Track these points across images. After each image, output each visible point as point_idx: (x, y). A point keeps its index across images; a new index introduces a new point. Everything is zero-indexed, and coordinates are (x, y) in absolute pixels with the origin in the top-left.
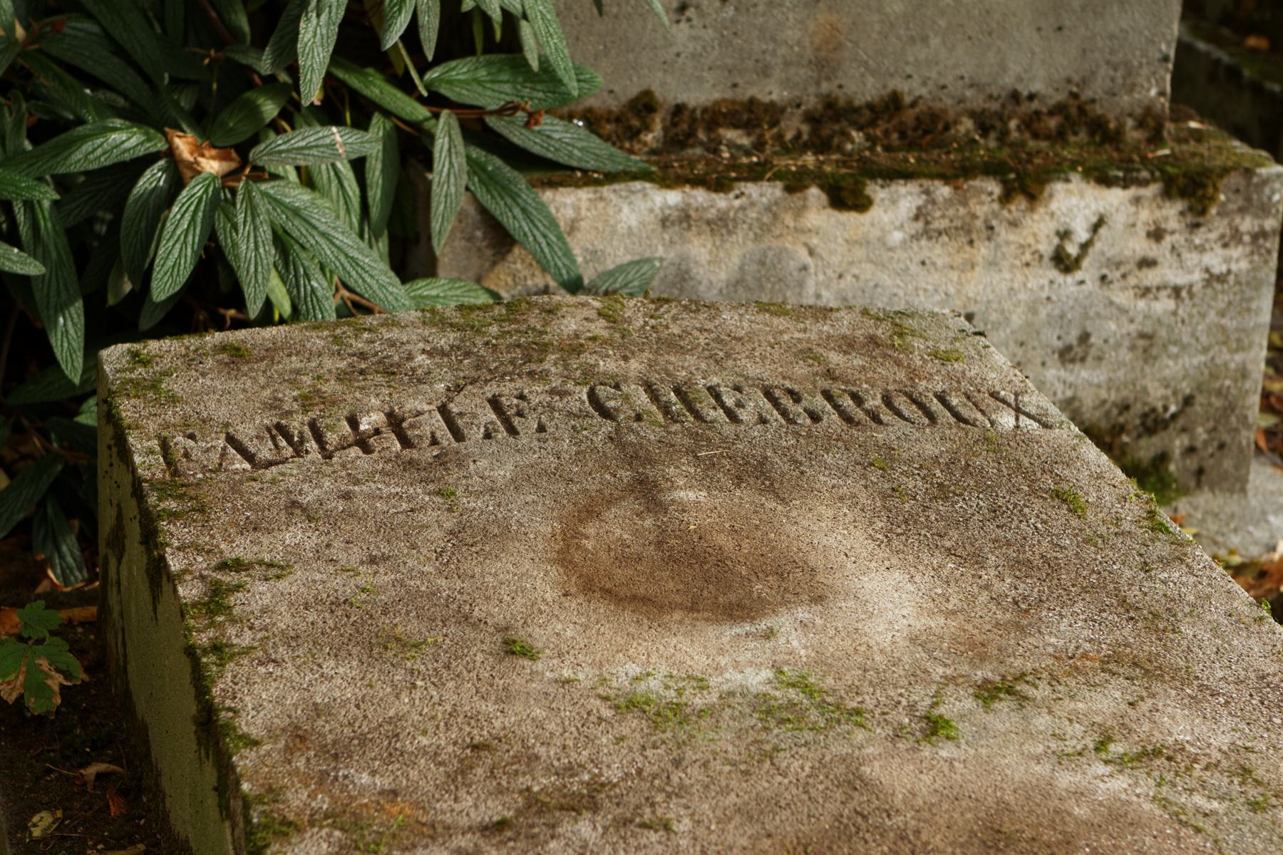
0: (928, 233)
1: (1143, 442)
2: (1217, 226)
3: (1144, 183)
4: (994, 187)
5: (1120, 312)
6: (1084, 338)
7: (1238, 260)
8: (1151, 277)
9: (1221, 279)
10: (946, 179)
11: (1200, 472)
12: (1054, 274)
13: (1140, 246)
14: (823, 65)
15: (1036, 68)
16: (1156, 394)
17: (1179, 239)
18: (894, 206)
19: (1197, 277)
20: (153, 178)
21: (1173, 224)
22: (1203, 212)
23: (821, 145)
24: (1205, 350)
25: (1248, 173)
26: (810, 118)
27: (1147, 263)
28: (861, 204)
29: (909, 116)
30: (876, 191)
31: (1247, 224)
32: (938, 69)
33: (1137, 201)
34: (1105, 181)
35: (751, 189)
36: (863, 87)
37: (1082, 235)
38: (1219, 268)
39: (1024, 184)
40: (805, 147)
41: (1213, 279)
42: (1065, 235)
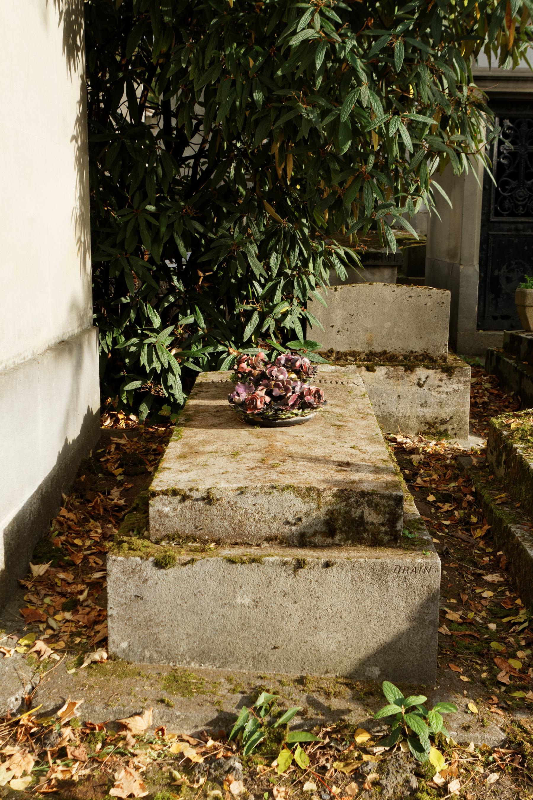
0: (388, 377)
1: (442, 426)
2: (455, 379)
3: (437, 369)
7: (461, 387)
8: (440, 389)
9: (457, 391)
10: (392, 366)
11: (455, 434)
12: (418, 387)
13: (438, 383)
15: (417, 346)
16: (444, 416)
18: (381, 371)
19: (451, 390)
20: (224, 355)
21: (445, 378)
22: (451, 376)
23: (369, 361)
24: (455, 406)
25: (462, 368)
26: (366, 355)
27: (439, 386)
28: (374, 371)
30: (376, 368)
31: (462, 379)
33: (436, 373)
34: (428, 368)
35: (350, 366)
36: (378, 349)
37: (424, 380)
38: (456, 388)
39: (410, 368)
40: (366, 361)
41: (455, 391)
42: (420, 379)
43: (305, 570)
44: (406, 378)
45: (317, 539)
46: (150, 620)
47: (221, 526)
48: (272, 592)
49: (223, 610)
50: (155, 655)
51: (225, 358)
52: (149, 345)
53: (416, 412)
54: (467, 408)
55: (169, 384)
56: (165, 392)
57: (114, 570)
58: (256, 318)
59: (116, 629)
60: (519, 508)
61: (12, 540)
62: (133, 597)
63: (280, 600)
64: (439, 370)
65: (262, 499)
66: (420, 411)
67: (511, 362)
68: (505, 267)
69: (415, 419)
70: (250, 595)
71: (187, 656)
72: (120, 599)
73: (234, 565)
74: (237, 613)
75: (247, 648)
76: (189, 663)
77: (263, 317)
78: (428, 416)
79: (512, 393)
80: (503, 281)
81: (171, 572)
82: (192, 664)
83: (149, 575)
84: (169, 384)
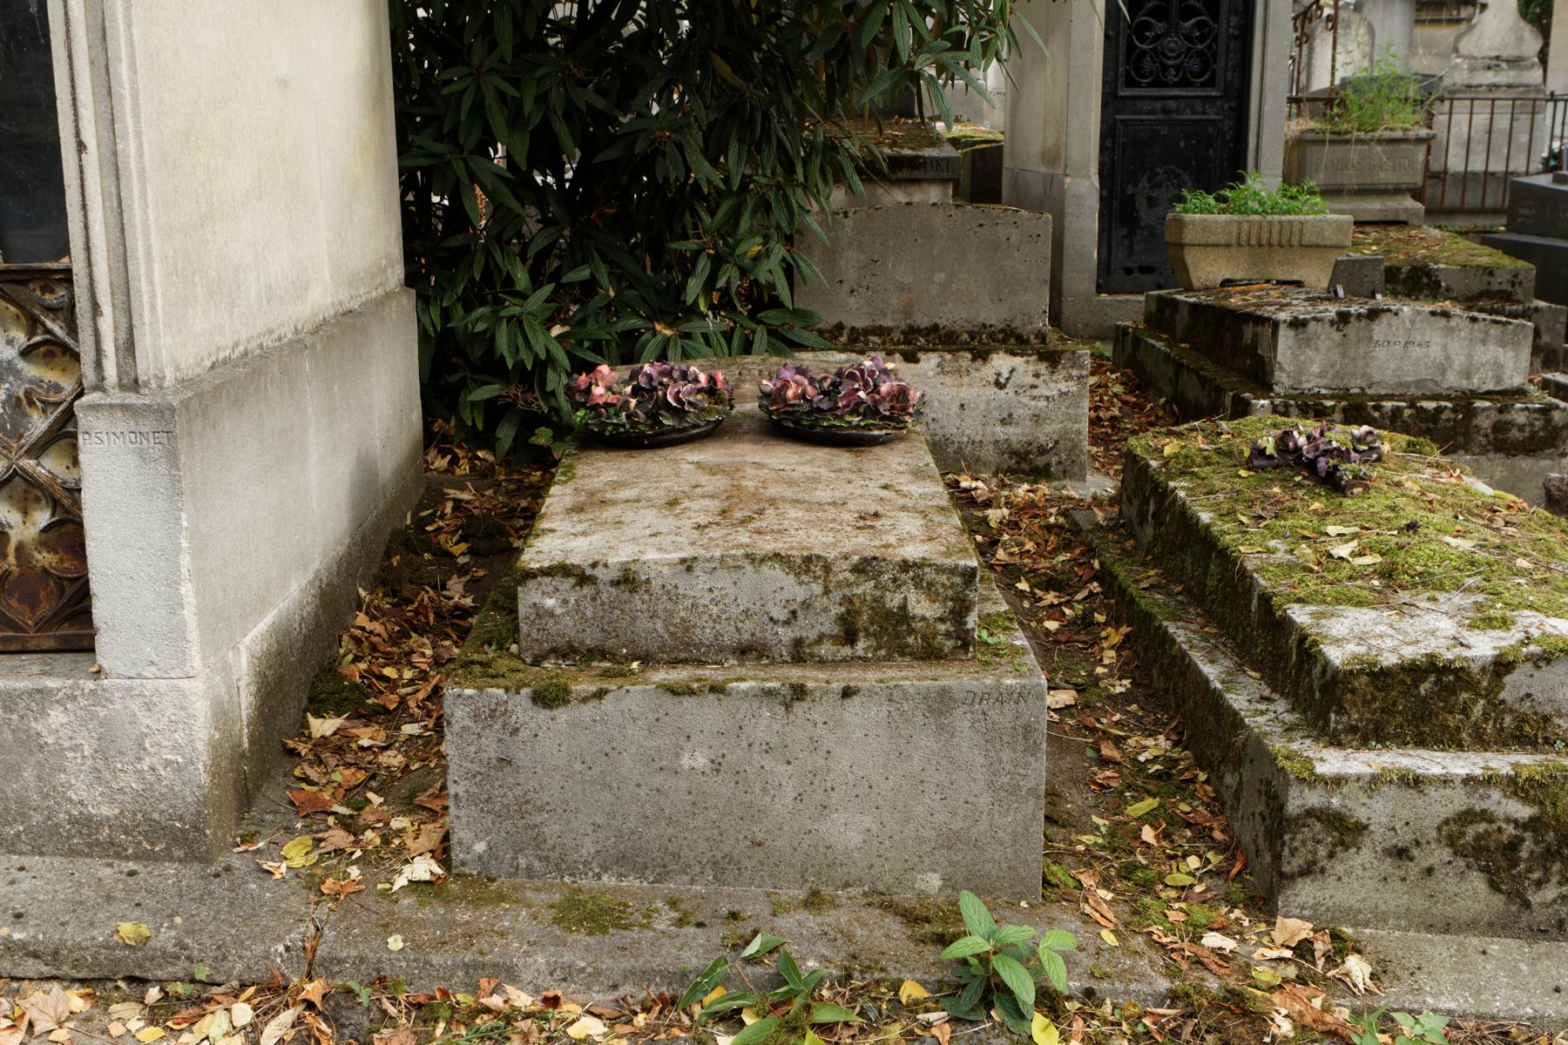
2: (1061, 373)
4: (969, 356)
5: (1025, 406)
6: (1010, 415)
7: (1072, 386)
8: (1036, 392)
9: (1066, 394)
13: (1031, 380)
14: (907, 312)
15: (993, 316)
16: (1043, 439)
17: (1046, 377)
23: (908, 343)
26: (903, 332)
27: (1033, 387)
28: (917, 361)
29: (942, 333)
30: (920, 355)
31: (1074, 372)
32: (952, 315)
34: (1014, 354)
36: (923, 322)
38: (1064, 390)
39: (981, 355)
41: (1062, 394)
42: (999, 375)
43: (805, 705)
44: (974, 373)
45: (826, 650)
46: (527, 802)
47: (651, 629)
48: (745, 744)
49: (658, 780)
50: (537, 864)
51: (648, 341)
52: (510, 319)
53: (994, 434)
54: (1084, 426)
55: (549, 388)
56: (542, 403)
57: (458, 713)
58: (704, 265)
59: (464, 820)
60: (1180, 593)
61: (270, 668)
62: (494, 761)
63: (759, 759)
64: (1034, 358)
65: (723, 580)
66: (1001, 432)
67: (1160, 345)
68: (1145, 179)
69: (991, 447)
70: (706, 751)
71: (594, 864)
72: (469, 765)
73: (676, 699)
74: (683, 785)
75: (703, 846)
76: (599, 876)
77: (718, 262)
78: (1014, 440)
79: (1162, 400)
80: (1141, 205)
81: (562, 715)
82: (605, 878)
83: (521, 720)
84: (549, 388)
